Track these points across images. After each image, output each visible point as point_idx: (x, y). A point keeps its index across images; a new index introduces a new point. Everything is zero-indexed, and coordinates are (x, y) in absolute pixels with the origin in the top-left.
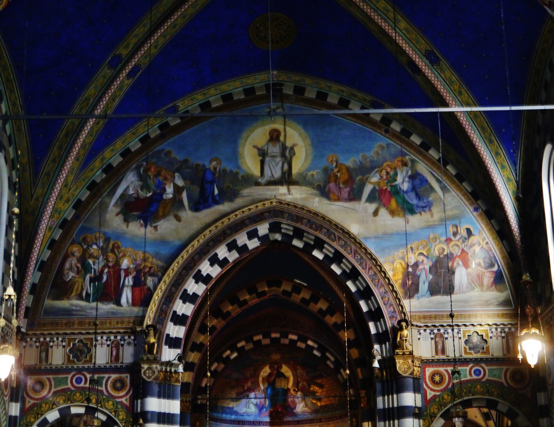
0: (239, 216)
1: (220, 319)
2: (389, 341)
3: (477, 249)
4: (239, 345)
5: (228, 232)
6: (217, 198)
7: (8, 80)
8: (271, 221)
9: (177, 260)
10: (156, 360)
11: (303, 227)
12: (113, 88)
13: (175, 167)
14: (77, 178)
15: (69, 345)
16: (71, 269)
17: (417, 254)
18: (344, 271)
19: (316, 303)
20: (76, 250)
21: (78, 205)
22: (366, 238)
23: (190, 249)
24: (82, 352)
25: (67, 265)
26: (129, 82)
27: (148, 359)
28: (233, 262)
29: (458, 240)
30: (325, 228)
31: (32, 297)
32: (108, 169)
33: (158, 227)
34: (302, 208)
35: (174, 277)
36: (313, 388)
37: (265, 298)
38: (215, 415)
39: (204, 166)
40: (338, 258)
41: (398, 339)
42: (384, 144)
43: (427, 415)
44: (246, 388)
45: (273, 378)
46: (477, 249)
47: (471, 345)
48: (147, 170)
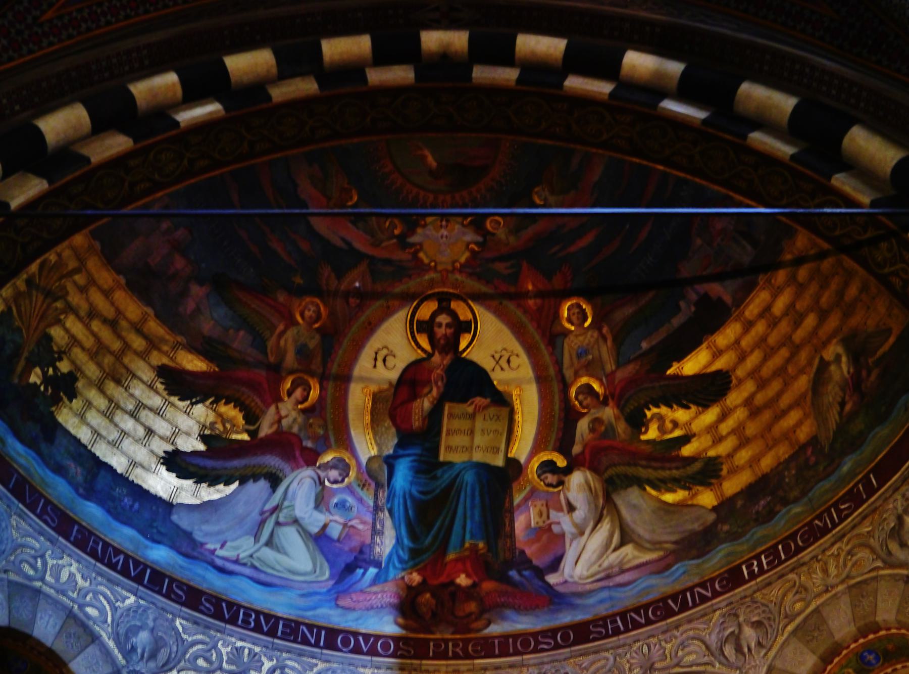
36: (661, 418)
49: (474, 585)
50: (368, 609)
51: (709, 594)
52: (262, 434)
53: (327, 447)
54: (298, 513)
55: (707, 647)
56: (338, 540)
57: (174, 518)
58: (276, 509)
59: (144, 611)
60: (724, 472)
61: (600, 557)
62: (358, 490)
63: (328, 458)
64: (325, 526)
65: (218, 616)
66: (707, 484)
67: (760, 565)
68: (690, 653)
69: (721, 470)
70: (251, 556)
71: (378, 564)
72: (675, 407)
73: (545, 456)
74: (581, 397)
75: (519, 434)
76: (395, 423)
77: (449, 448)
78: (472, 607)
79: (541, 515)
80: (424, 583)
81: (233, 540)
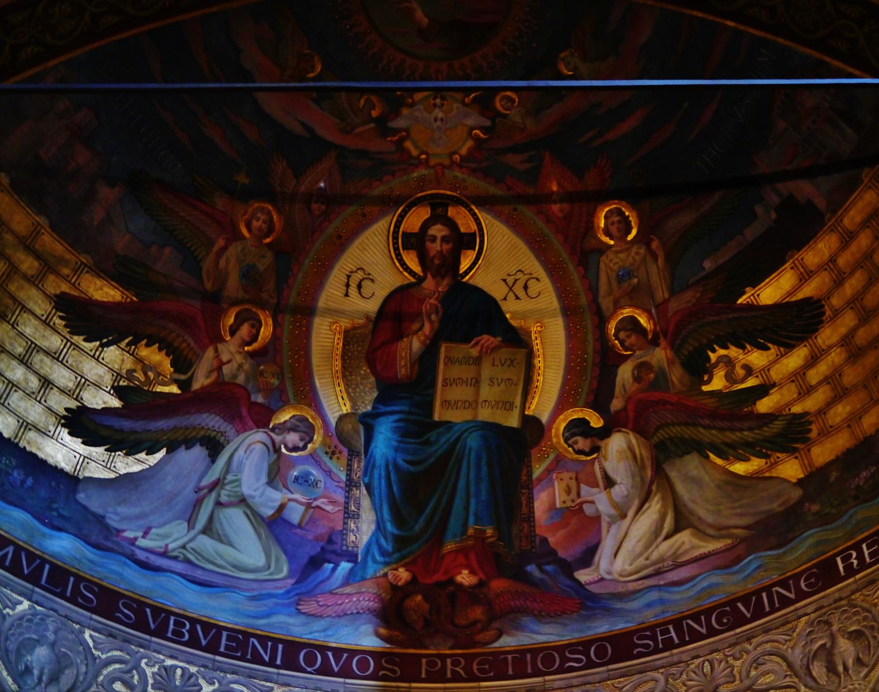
36: (729, 362)
45: (416, 344)
49: (481, 584)
50: (339, 616)
51: (792, 596)
52: (196, 386)
53: (284, 403)
54: (246, 490)
55: (790, 666)
56: (299, 526)
57: (81, 497)
58: (216, 485)
59: (42, 620)
60: (813, 434)
61: (647, 548)
62: (326, 459)
63: (285, 416)
64: (282, 507)
65: (140, 625)
66: (791, 451)
67: (860, 556)
68: (767, 673)
69: (810, 430)
70: (184, 547)
71: (351, 557)
72: (748, 346)
73: (575, 414)
74: (622, 335)
75: (540, 384)
76: (374, 372)
77: (446, 404)
78: (478, 613)
79: (568, 491)
80: (413, 581)
81: (160, 526)
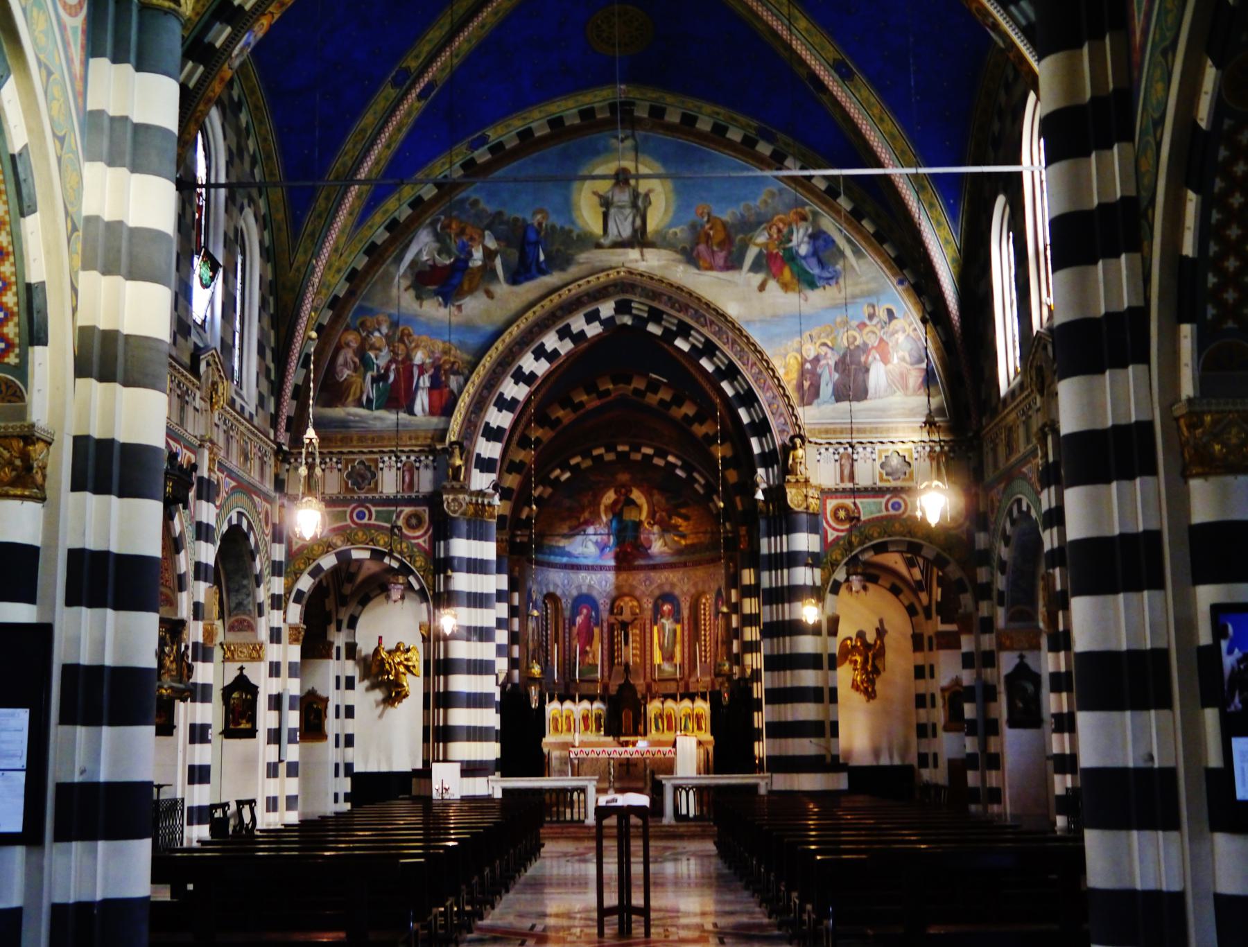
0: (573, 292)
1: (547, 428)
2: (778, 463)
3: (901, 337)
4: (573, 462)
5: (559, 313)
6: (543, 266)
7: (257, 107)
8: (618, 298)
9: (489, 353)
10: (464, 489)
11: (661, 307)
12: (399, 115)
13: (486, 221)
14: (350, 238)
15: (347, 468)
16: (346, 364)
17: (818, 344)
18: (718, 368)
19: (680, 405)
20: (352, 339)
21: (353, 276)
22: (748, 322)
23: (507, 338)
24: (363, 477)
25: (341, 360)
26: (421, 105)
27: (453, 487)
28: (566, 354)
29: (875, 326)
30: (692, 308)
31: (295, 403)
32: (393, 226)
33: (463, 307)
34: (661, 281)
35: (485, 376)
37: (609, 399)
38: (540, 557)
39: (524, 220)
40: (710, 349)
41: (790, 461)
42: (775, 189)
43: (826, 563)
44: (582, 520)
45: (619, 507)
46: (901, 337)
47: (889, 469)
48: (446, 227)
